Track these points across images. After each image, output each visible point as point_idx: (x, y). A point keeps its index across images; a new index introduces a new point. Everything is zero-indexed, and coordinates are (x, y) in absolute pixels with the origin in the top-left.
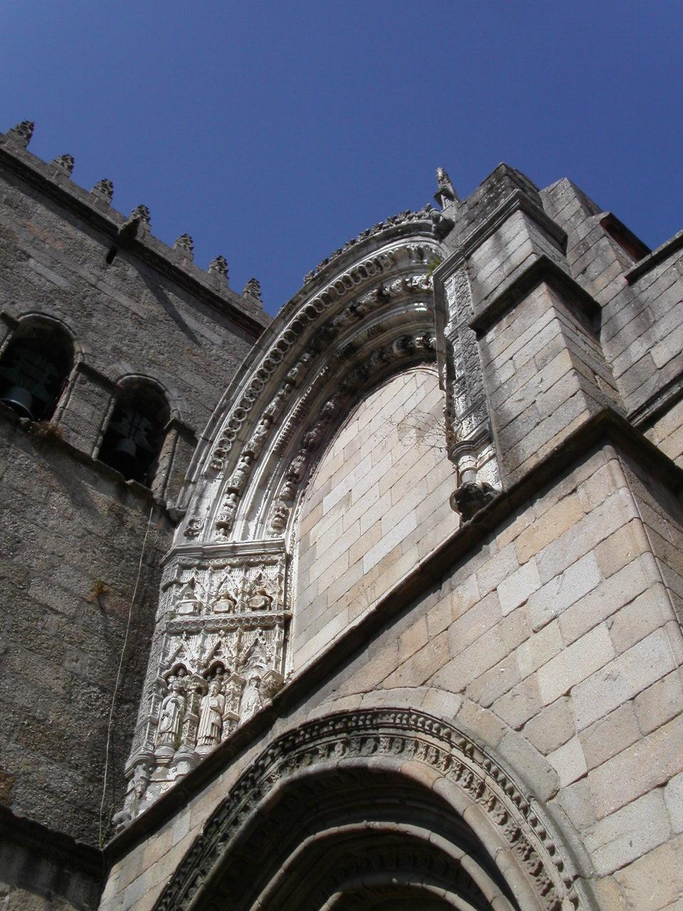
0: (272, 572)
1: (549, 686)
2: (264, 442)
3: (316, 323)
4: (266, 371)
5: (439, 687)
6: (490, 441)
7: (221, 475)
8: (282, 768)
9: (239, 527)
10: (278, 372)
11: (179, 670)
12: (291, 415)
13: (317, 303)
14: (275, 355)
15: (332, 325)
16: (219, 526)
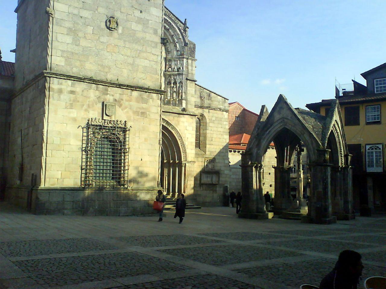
1: (187, 137)
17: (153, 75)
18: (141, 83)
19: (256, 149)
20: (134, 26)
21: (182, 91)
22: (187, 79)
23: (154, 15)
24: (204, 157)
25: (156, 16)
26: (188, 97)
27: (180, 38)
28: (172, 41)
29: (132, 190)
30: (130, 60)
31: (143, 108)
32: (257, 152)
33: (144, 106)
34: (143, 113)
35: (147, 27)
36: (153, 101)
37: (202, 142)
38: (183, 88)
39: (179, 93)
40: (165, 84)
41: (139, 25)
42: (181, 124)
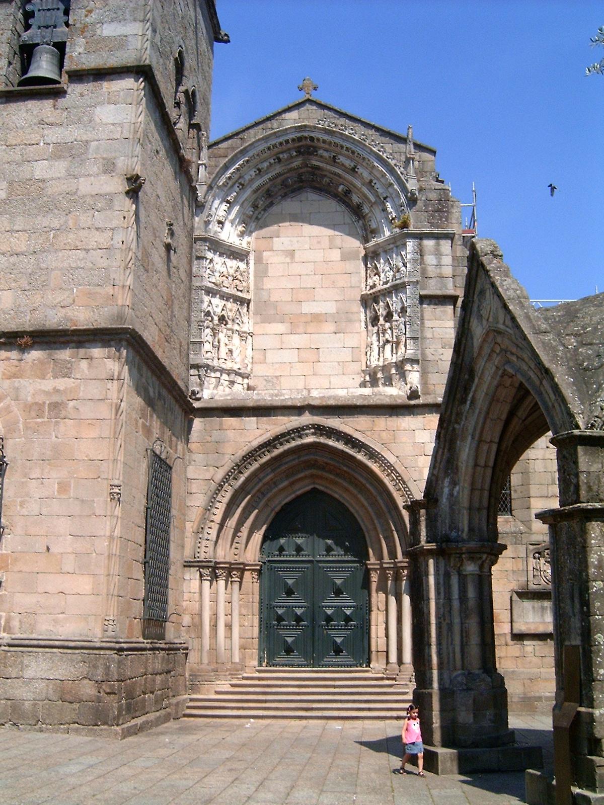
0: (242, 266)
2: (252, 181)
3: (309, 142)
4: (272, 147)
5: (388, 450)
6: (418, 364)
7: (225, 189)
8: (313, 434)
9: (227, 225)
10: (276, 150)
11: (208, 314)
12: (270, 176)
13: (318, 140)
14: (281, 144)
15: (317, 152)
16: (220, 222)
17: (98, 289)
18: (54, 319)
19: (447, 481)
20: (40, 170)
21: (405, 334)
22: (423, 299)
23: (106, 124)
24: (524, 541)
25: (113, 124)
26: (428, 351)
27: (391, 185)
28: (373, 199)
29: (10, 645)
30: (28, 263)
31: (56, 391)
32: (451, 495)
33: (62, 383)
34: (56, 407)
35: (83, 162)
36: (90, 366)
37: (515, 491)
38: (407, 326)
39: (398, 343)
40: (367, 327)
41: (57, 163)
42: (404, 437)
